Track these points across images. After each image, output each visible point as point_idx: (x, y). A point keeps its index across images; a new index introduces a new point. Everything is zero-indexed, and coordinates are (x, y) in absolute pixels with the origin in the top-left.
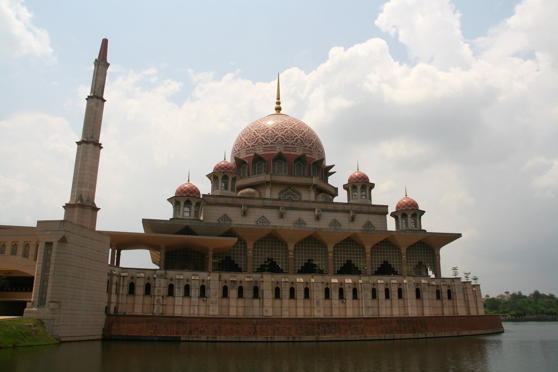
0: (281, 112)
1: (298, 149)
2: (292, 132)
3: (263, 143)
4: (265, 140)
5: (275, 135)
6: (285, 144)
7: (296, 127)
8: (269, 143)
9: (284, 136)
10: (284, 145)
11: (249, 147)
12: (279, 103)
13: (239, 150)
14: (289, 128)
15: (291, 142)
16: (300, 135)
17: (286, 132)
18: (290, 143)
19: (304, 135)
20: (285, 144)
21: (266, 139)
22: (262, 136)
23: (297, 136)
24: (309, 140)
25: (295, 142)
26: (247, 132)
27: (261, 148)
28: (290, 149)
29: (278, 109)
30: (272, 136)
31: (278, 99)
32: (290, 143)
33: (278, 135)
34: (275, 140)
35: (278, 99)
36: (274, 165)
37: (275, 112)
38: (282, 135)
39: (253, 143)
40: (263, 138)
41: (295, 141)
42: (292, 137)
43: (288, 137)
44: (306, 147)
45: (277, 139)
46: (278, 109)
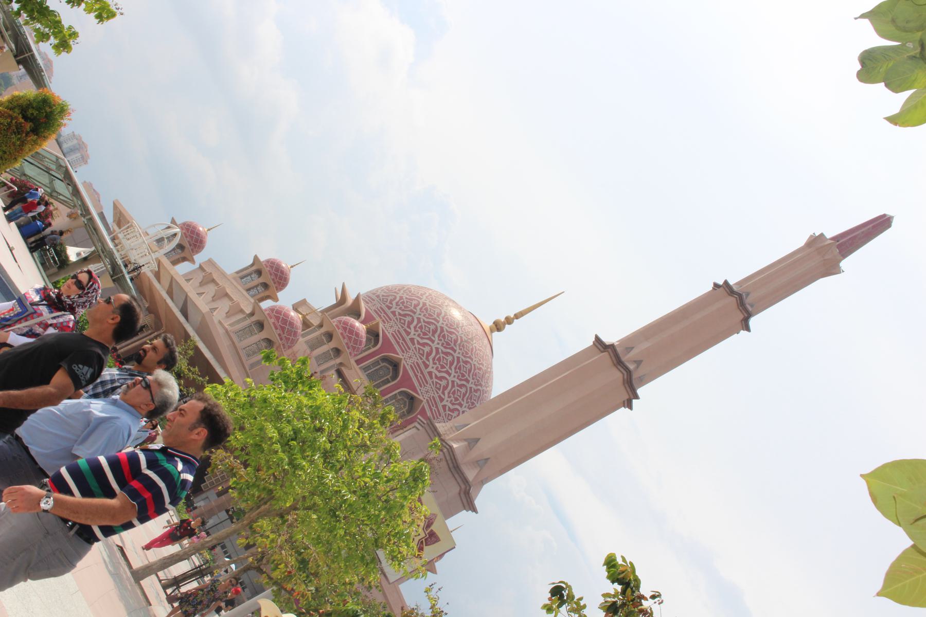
0: (496, 334)
1: (428, 387)
2: (452, 364)
3: (405, 327)
4: (412, 326)
5: (429, 339)
6: (424, 362)
7: (481, 372)
8: (411, 336)
9: (437, 352)
10: (420, 362)
11: (389, 308)
12: (509, 321)
13: (378, 296)
14: (456, 355)
15: (434, 371)
16: (455, 379)
17: (447, 354)
18: (430, 369)
19: (461, 386)
20: (424, 362)
21: (415, 327)
22: (419, 319)
23: (449, 374)
24: (456, 399)
25: (436, 377)
26: (407, 289)
27: (396, 328)
28: (419, 375)
29: (498, 326)
30: (425, 334)
31: (517, 316)
32: (430, 369)
33: (433, 341)
34: (421, 341)
35: (517, 316)
36: (376, 363)
37: (488, 323)
38: (437, 349)
39: (398, 311)
40: (415, 322)
41: (439, 375)
42: (443, 367)
43: (439, 359)
44: (442, 400)
45: (424, 345)
46: (498, 326)
